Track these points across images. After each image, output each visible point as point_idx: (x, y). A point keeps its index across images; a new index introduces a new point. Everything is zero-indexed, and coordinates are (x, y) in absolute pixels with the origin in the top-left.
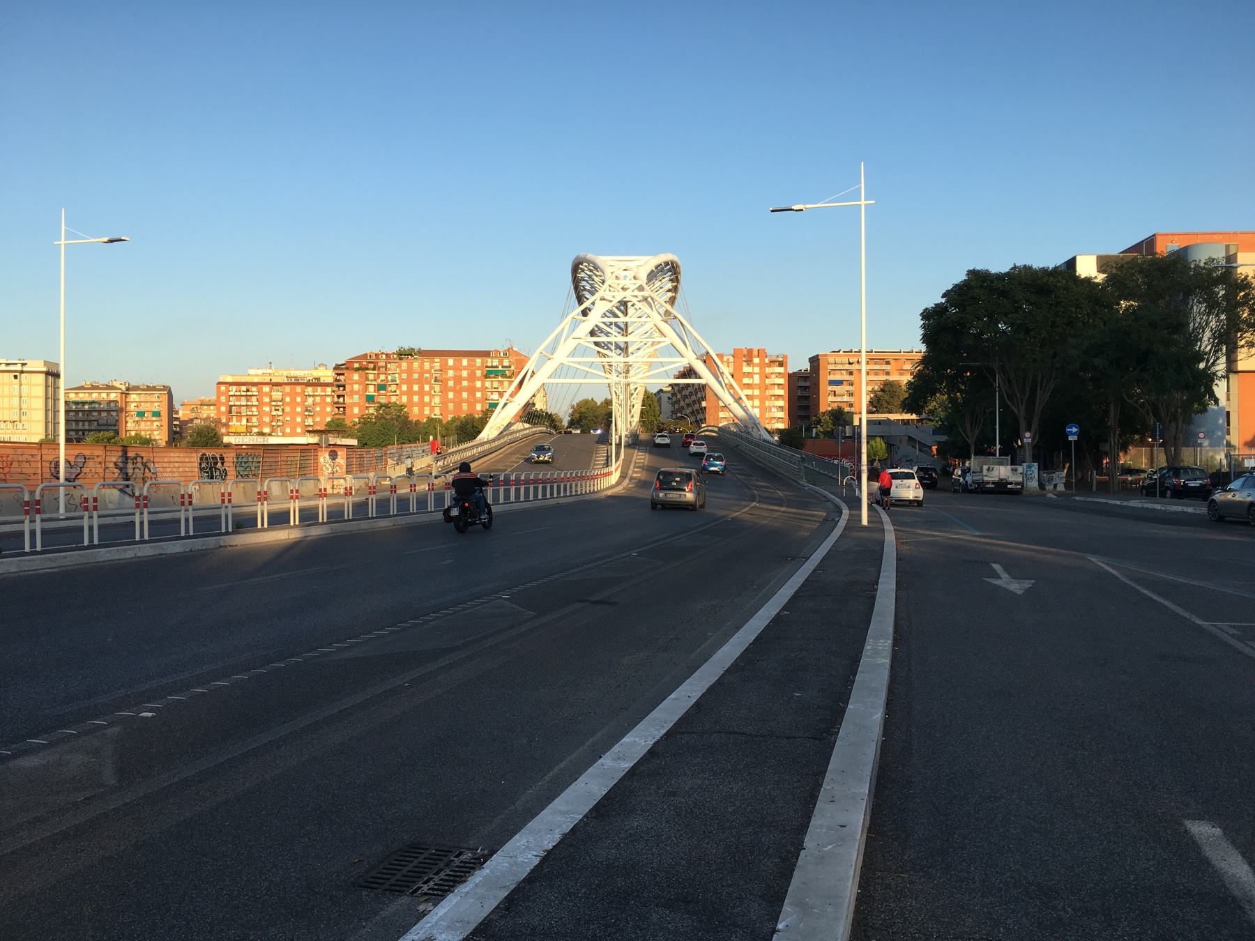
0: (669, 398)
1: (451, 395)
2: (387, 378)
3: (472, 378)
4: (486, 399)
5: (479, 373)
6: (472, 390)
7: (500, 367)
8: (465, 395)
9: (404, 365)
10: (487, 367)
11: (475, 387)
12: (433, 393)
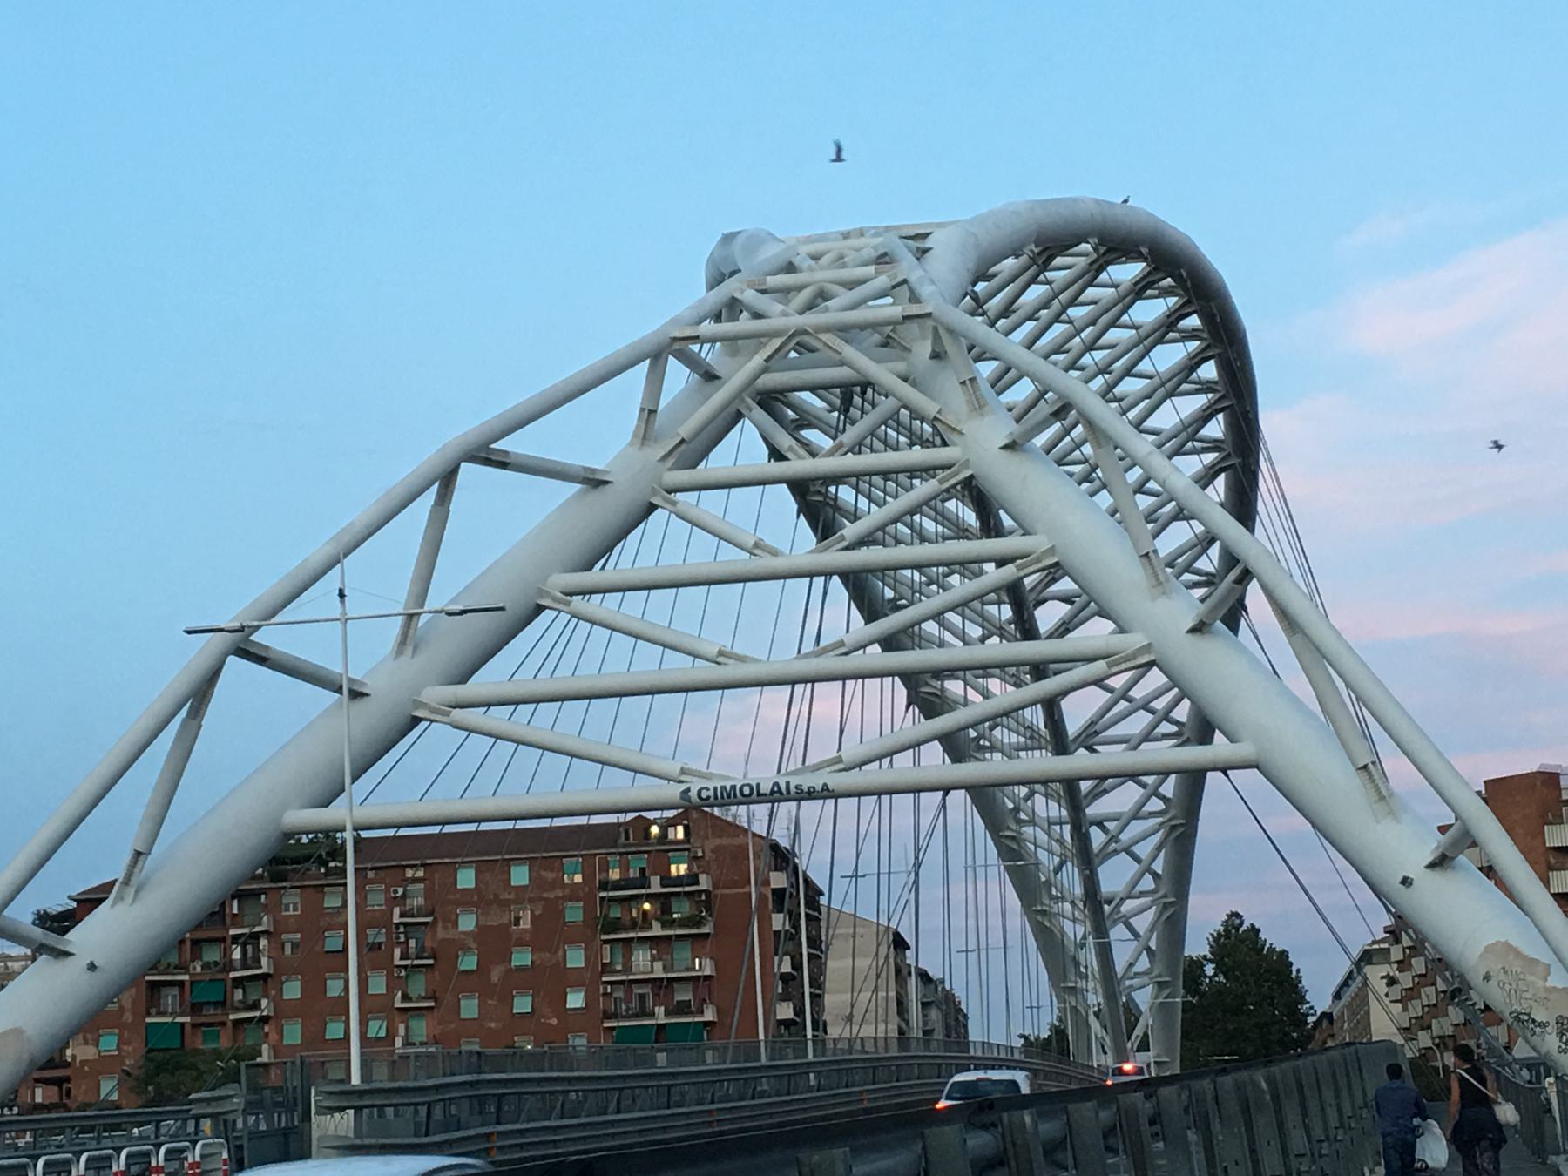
0: (1392, 981)
1: (470, 1008)
2: (227, 953)
3: (550, 932)
4: (608, 1016)
5: (574, 913)
6: (549, 980)
7: (655, 881)
8: (523, 1004)
9: (292, 902)
10: (605, 885)
11: (561, 966)
12: (398, 1004)
